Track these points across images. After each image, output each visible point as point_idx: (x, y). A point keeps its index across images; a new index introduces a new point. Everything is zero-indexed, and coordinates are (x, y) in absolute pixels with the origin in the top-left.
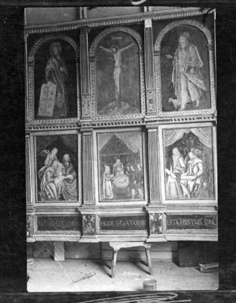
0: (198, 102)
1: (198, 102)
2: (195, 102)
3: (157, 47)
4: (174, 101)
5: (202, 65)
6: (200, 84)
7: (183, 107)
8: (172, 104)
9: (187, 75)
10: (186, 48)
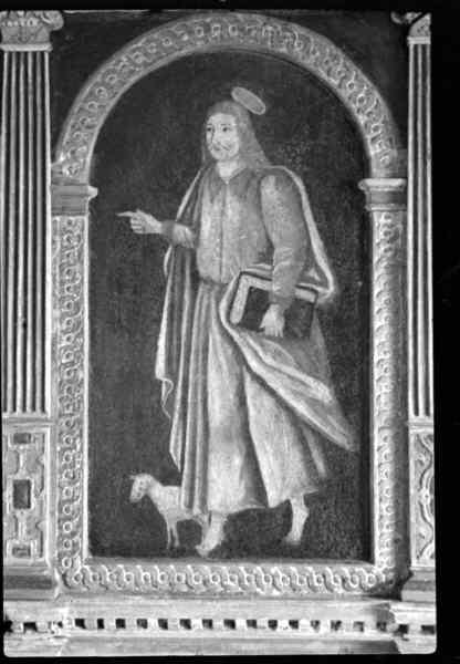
0: (300, 516)
1: (300, 516)
2: (286, 510)
3: (74, 160)
4: (169, 501)
5: (330, 290)
6: (313, 403)
7: (213, 538)
8: (148, 513)
9: (246, 341)
10: (248, 184)
